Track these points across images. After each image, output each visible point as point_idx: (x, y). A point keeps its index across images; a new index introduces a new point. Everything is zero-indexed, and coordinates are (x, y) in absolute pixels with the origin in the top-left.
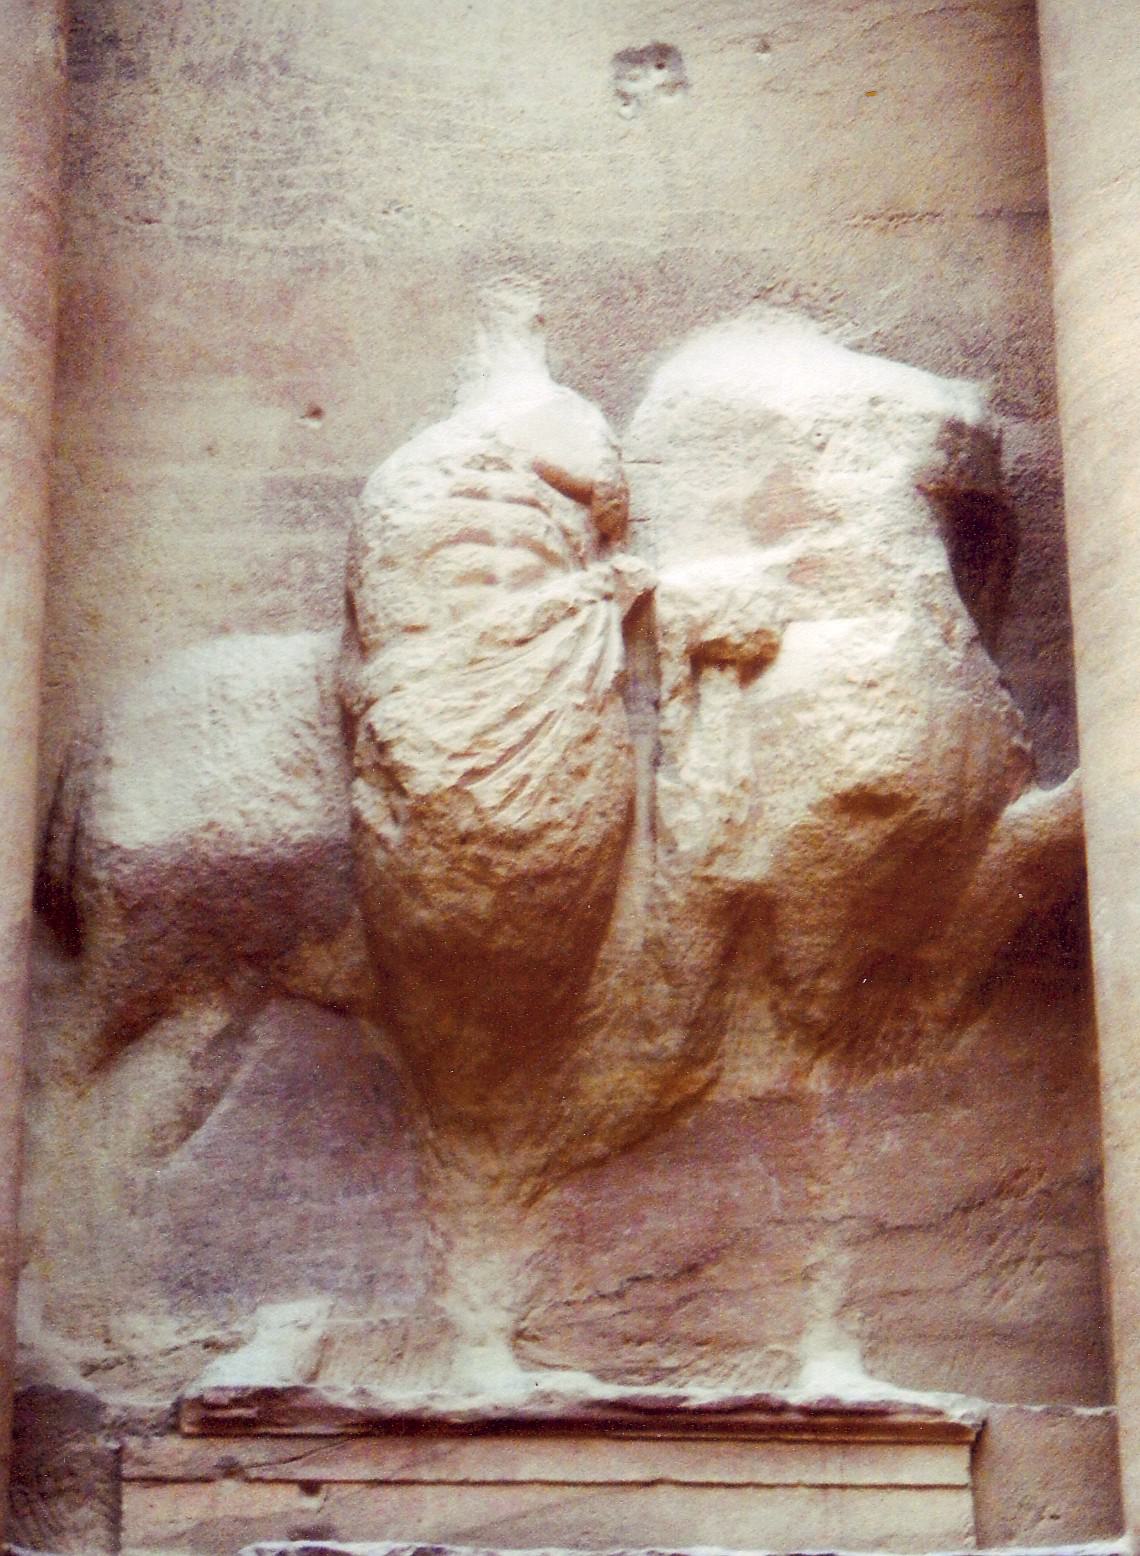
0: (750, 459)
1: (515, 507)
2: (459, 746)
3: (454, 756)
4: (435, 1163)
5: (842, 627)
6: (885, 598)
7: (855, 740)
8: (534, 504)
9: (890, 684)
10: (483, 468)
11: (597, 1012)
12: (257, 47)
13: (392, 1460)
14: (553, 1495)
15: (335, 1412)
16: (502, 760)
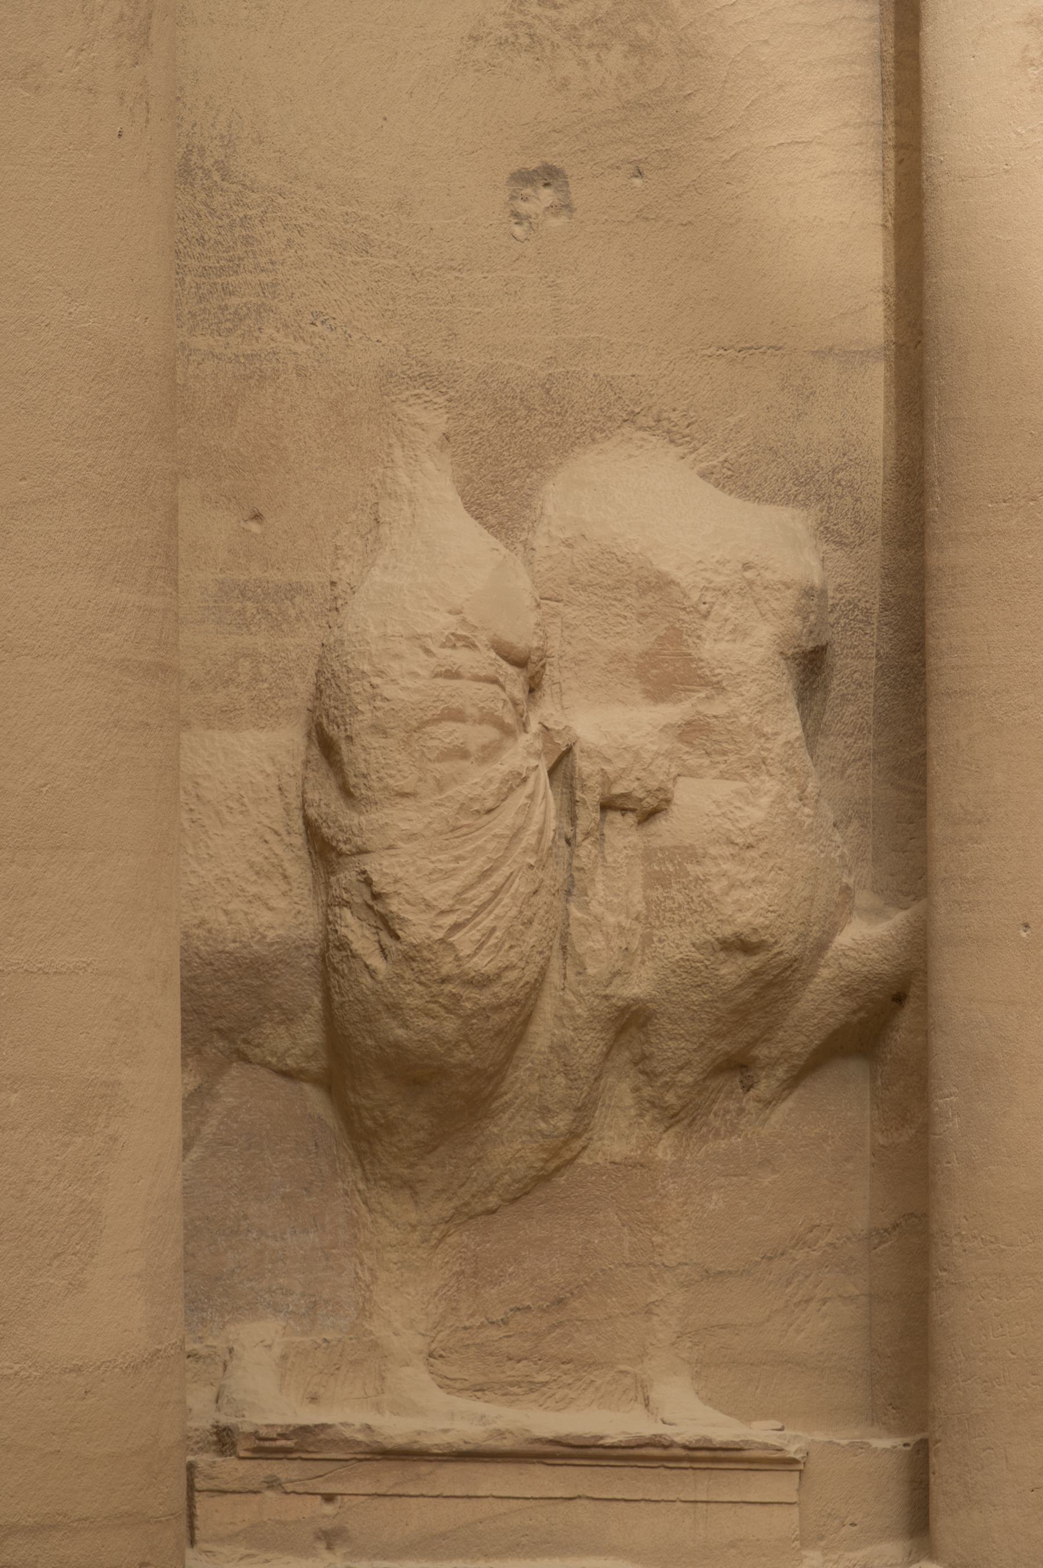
0: (644, 615)
1: (480, 685)
2: (444, 904)
3: (442, 913)
4: (363, 1209)
5: (725, 789)
6: (759, 765)
7: (735, 894)
8: (495, 681)
9: (764, 846)
10: (454, 646)
11: (506, 1098)
12: (202, 150)
13: (389, 1477)
14: (504, 1506)
15: (349, 1443)
16: (476, 914)
